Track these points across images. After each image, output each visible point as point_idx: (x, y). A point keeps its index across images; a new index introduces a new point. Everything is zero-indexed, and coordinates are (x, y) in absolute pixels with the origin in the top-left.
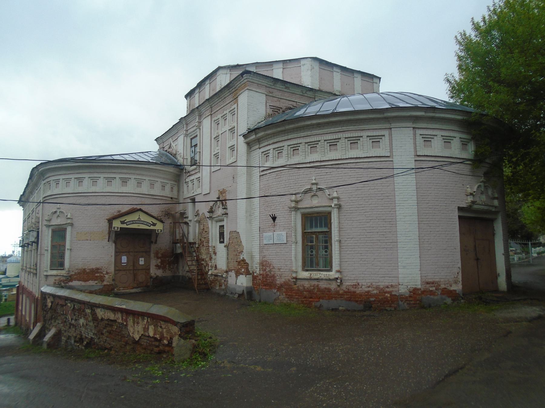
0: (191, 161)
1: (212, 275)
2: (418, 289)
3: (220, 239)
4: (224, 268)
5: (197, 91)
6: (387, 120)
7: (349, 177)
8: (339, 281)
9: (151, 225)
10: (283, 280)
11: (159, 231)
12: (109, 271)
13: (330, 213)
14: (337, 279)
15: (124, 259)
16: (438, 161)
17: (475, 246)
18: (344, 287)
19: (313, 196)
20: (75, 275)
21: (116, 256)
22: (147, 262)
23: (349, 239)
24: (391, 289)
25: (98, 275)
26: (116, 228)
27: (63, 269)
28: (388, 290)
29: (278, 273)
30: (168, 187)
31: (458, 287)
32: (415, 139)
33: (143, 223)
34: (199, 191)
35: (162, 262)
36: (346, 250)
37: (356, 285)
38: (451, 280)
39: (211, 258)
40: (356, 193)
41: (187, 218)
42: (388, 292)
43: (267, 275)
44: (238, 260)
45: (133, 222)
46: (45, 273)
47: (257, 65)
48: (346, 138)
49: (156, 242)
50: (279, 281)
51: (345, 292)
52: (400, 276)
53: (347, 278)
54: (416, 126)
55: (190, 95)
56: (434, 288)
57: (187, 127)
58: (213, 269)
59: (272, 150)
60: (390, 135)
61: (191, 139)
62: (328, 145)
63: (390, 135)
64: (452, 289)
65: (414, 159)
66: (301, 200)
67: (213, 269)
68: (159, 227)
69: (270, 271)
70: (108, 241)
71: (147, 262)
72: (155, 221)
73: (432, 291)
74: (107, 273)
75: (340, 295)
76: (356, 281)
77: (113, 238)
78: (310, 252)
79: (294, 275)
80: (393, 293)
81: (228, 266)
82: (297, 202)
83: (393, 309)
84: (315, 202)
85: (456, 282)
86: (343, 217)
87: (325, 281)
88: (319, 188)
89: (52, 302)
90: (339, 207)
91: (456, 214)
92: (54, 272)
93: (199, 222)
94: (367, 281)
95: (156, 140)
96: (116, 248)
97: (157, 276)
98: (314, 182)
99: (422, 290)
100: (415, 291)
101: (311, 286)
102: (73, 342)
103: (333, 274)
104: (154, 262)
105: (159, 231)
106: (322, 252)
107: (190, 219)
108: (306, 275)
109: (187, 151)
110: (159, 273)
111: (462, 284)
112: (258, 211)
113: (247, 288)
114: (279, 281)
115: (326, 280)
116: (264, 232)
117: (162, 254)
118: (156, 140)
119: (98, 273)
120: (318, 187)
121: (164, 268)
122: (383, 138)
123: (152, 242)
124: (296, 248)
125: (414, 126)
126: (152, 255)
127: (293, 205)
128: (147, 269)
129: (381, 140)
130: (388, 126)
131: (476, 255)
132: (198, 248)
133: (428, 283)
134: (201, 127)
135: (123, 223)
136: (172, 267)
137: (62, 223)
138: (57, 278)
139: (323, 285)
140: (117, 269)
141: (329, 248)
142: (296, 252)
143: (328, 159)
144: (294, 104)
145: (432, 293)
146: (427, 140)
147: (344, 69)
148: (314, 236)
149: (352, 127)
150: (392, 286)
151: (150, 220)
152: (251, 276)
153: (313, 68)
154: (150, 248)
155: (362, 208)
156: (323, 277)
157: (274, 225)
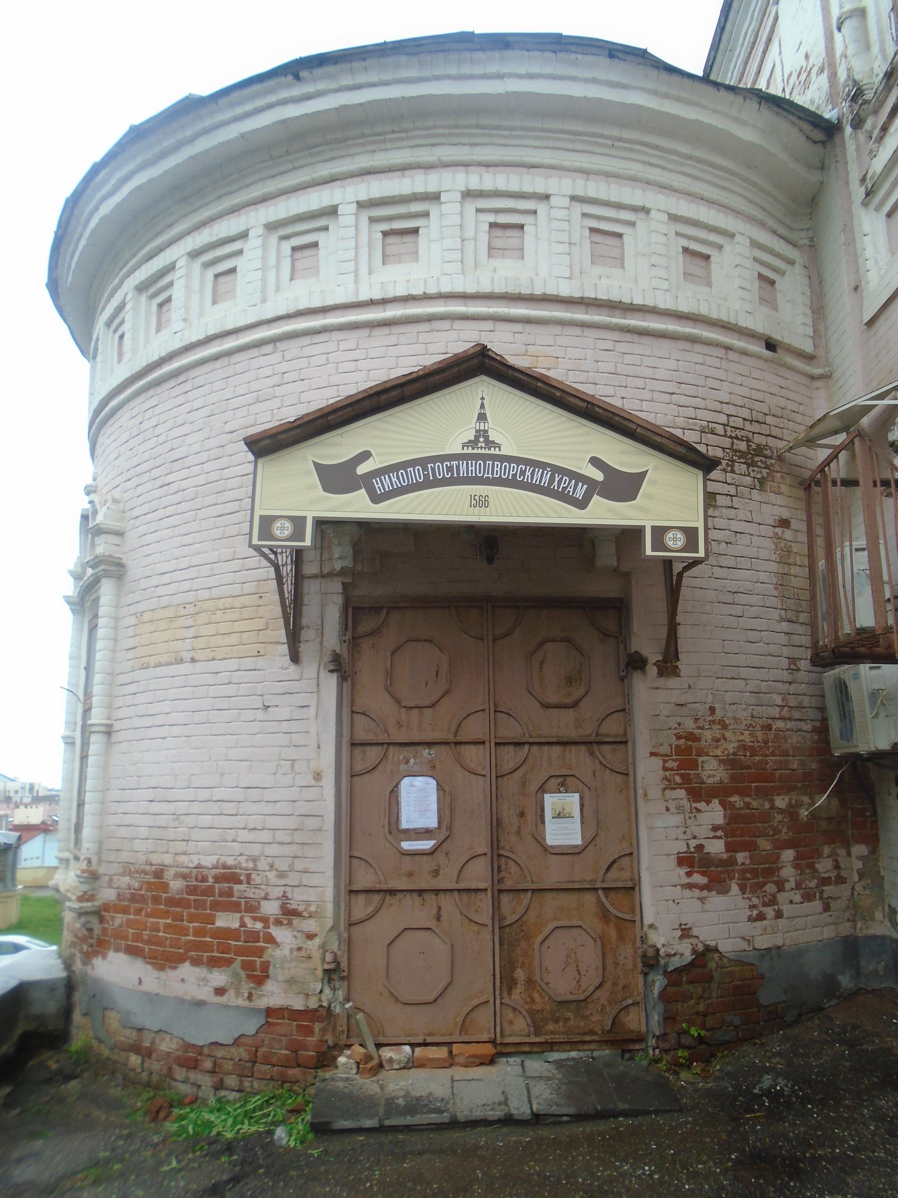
9: (593, 487)
11: (675, 541)
12: (298, 898)
33: (523, 474)
35: (737, 830)
45: (430, 473)
49: (669, 665)
70: (295, 658)
72: (623, 455)
77: (332, 639)
96: (350, 708)
104: (665, 830)
105: (675, 541)
110: (724, 923)
117: (730, 762)
119: (234, 907)
121: (760, 879)
123: (637, 663)
126: (648, 771)
135: (337, 478)
136: (824, 866)
140: (365, 879)
154: (625, 711)
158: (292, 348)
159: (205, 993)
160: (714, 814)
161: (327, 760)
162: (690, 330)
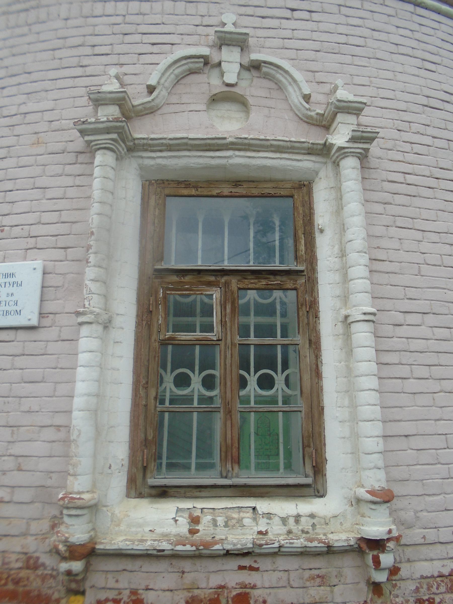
7: (393, 48)
8: (387, 559)
14: (377, 545)
23: (411, 319)
36: (404, 371)
40: (423, 118)
66: (150, 111)
79: (77, 532)
82: (129, 113)
87: (292, 564)
88: (255, 66)
103: (332, 514)
115: (304, 553)
142: (100, 381)
148: (216, 294)
156: (277, 534)
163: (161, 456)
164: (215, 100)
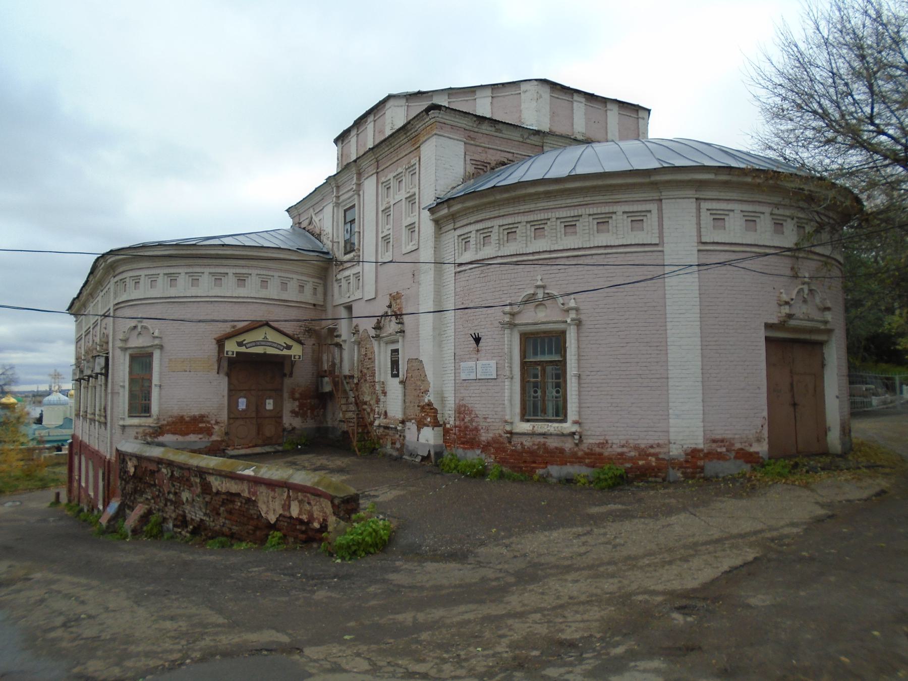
0: (345, 247)
1: (379, 426)
2: (701, 450)
3: (392, 370)
4: (400, 416)
5: (354, 133)
6: (655, 185)
8: (577, 437)
10: (491, 435)
11: (297, 357)
12: (219, 420)
13: (563, 333)
14: (574, 433)
15: (242, 404)
16: (734, 251)
17: (792, 384)
18: (584, 447)
19: (537, 306)
20: (166, 425)
21: (230, 396)
22: (278, 405)
24: (657, 450)
25: (204, 425)
26: (230, 353)
27: (150, 416)
28: (652, 451)
29: (483, 424)
30: (308, 289)
31: (762, 448)
32: (699, 217)
33: (273, 345)
34: (358, 295)
35: (301, 406)
37: (602, 445)
38: (751, 436)
39: (378, 401)
41: (339, 336)
42: (654, 455)
43: (466, 427)
44: (422, 404)
45: (256, 344)
46: (121, 423)
47: (450, 92)
48: (590, 215)
49: (291, 375)
50: (484, 437)
51: (587, 454)
52: (671, 430)
53: (589, 433)
54: (701, 197)
55: (341, 139)
56: (724, 449)
57: (338, 191)
58: (382, 417)
59: (474, 232)
60: (660, 210)
61: (345, 211)
62: (563, 225)
63: (660, 210)
64: (752, 450)
65: (696, 249)
67: (382, 417)
68: (296, 351)
69: (472, 421)
71: (278, 405)
72: (290, 342)
73: (721, 453)
74: (217, 423)
75: (578, 458)
76: (602, 438)
77: (226, 369)
78: (532, 393)
79: (508, 428)
80: (661, 456)
81: (404, 413)
82: (513, 315)
83: (659, 480)
84: (541, 315)
85: (759, 440)
86: (584, 339)
89: (136, 467)
90: (579, 323)
91: (762, 334)
92: (136, 421)
93: (359, 343)
94: (621, 437)
95: (287, 211)
96: (230, 383)
97: (294, 429)
98: (539, 283)
99: (705, 451)
100: (694, 453)
101: (534, 444)
102: (171, 525)
103: (567, 427)
104: (289, 406)
105: (297, 357)
106: (551, 392)
107: (343, 338)
108: (526, 427)
109: (338, 230)
110: (297, 423)
111: (770, 443)
112: (453, 327)
113: (435, 446)
114: (484, 437)
115: (557, 435)
116: (462, 360)
117: (300, 394)
118: (287, 211)
120: (546, 291)
121: (304, 416)
122: (648, 215)
123: (285, 375)
124: (511, 385)
125: (697, 196)
126: (286, 395)
127: (507, 319)
128: (277, 417)
129: (645, 218)
130: (656, 195)
131: (793, 396)
132: (357, 384)
133: (714, 441)
134: (361, 193)
136: (315, 413)
137: (145, 345)
138: (141, 430)
139: (552, 443)
140: (232, 416)
141: (562, 385)
142: (511, 393)
143: (561, 248)
144: (510, 156)
145: (720, 456)
146: (719, 219)
147: (591, 97)
148: (539, 368)
149: (601, 197)
150: (659, 445)
151: (282, 340)
152: (441, 429)
153: (541, 97)
154: (282, 384)
155: (614, 326)
156: (552, 430)
157: (478, 351)
158: (216, 304)
159: (197, 439)
160: (297, 403)
161: (226, 393)
162: (300, 305)
163: (530, 411)
164: (537, 306)
